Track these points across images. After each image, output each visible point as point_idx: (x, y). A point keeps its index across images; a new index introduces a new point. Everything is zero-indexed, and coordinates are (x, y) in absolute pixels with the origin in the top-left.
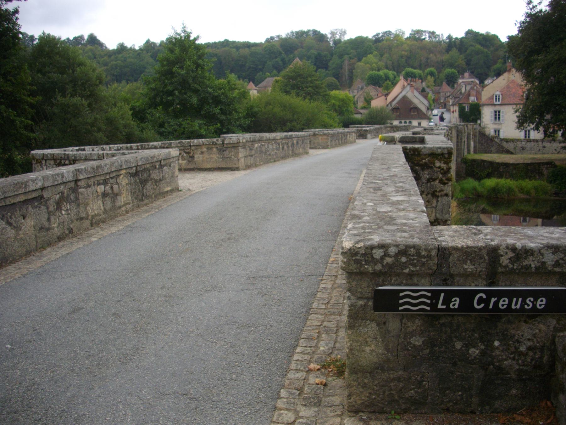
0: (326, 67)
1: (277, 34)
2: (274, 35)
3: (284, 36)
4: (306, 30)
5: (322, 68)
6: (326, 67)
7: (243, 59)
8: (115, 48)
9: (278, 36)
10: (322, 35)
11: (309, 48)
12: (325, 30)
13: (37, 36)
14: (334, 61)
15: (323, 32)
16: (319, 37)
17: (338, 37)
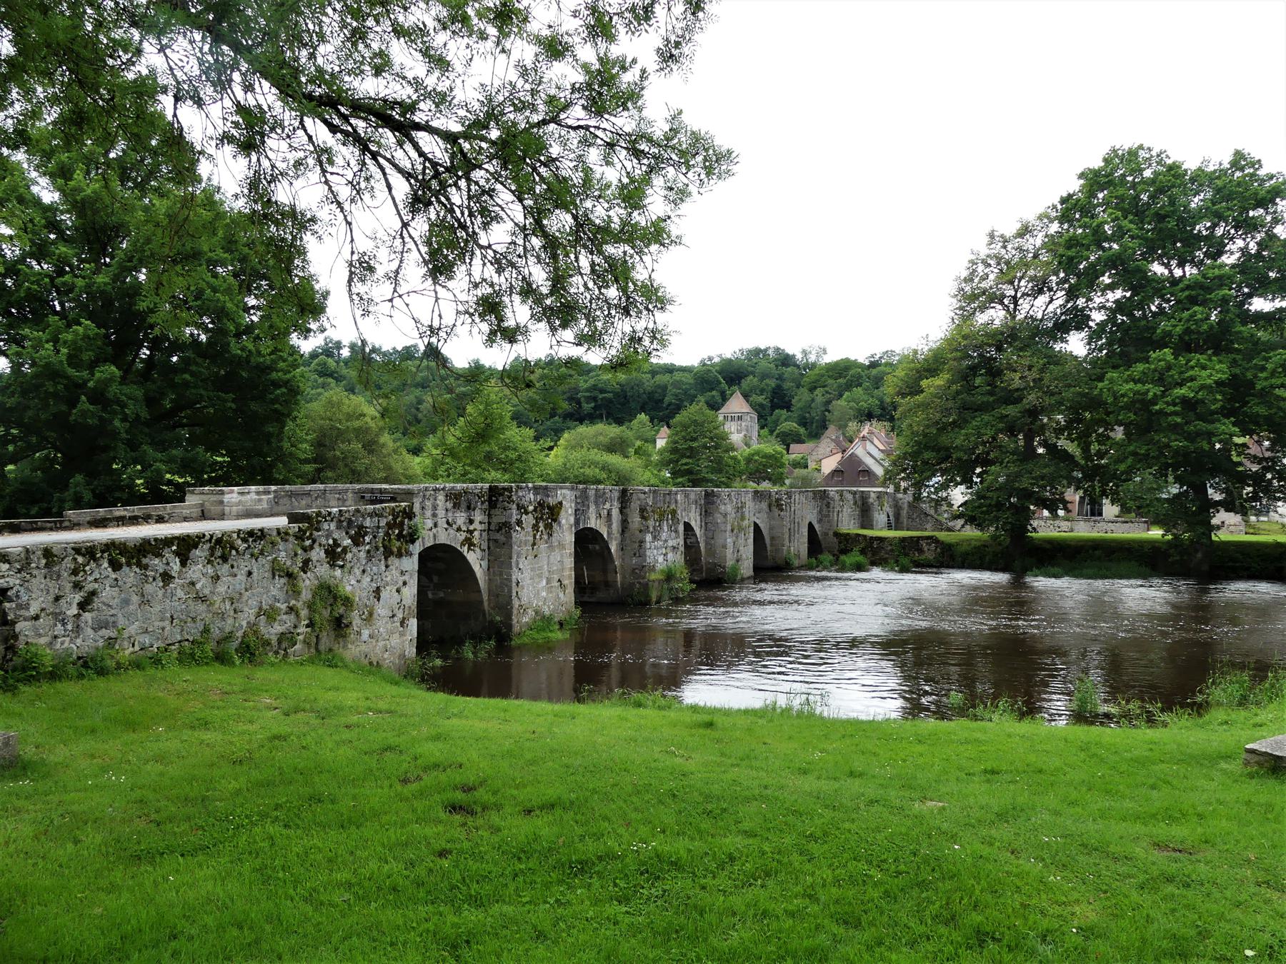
0: (788, 406)
1: (719, 353)
2: (713, 354)
3: (728, 355)
4: (763, 347)
5: (782, 408)
6: (788, 406)
7: (659, 391)
8: (467, 366)
9: (720, 356)
10: (788, 355)
11: (764, 376)
12: (793, 349)
13: (346, 342)
14: (801, 398)
15: (790, 351)
16: (785, 360)
17: (812, 358)
